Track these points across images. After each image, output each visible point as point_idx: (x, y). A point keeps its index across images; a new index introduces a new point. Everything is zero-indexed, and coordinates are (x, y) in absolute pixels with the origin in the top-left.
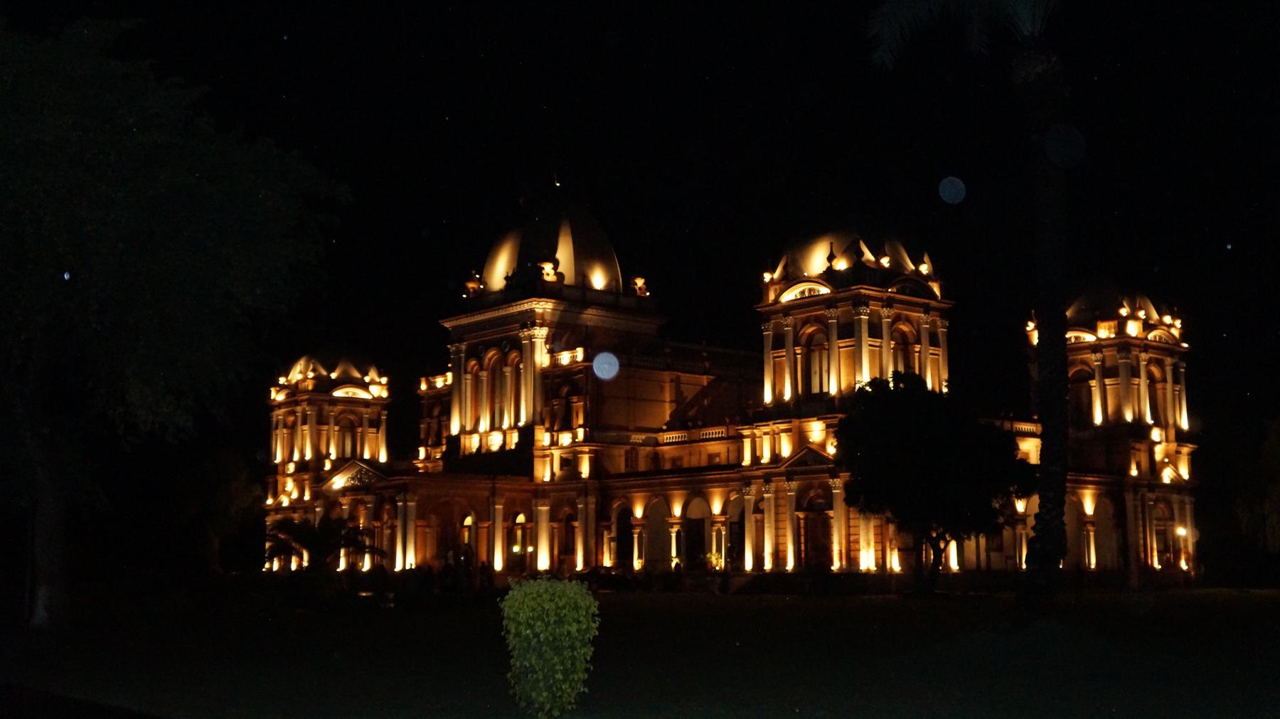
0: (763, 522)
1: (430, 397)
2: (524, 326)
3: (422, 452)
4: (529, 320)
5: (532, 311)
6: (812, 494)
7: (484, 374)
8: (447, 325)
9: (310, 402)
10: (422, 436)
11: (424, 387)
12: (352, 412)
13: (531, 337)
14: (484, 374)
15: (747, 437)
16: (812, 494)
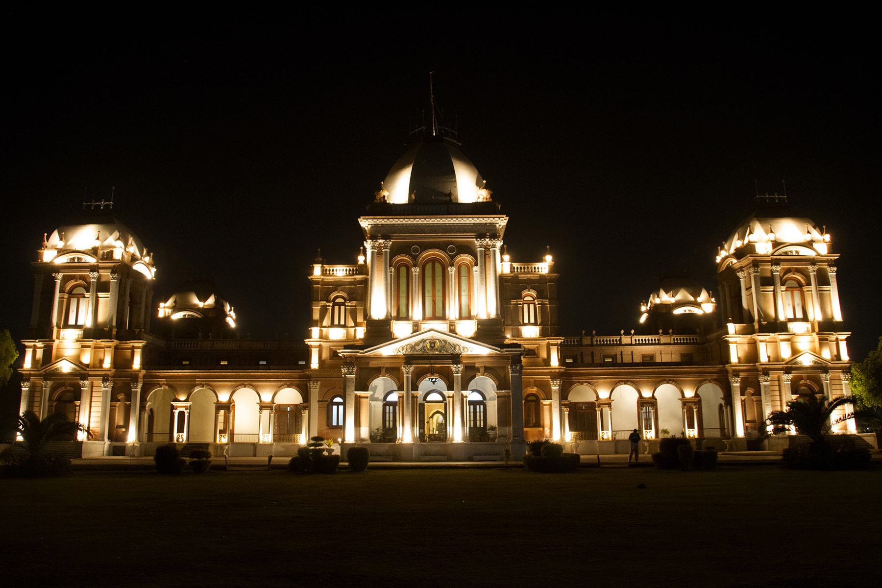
0: (761, 401)
1: (324, 283)
2: (481, 236)
3: (315, 331)
4: (490, 232)
5: (493, 225)
6: (802, 382)
7: (416, 271)
8: (365, 223)
9: (114, 271)
10: (316, 316)
11: (317, 270)
12: (798, 271)
13: (487, 248)
14: (416, 271)
15: (732, 343)
16: (802, 382)
